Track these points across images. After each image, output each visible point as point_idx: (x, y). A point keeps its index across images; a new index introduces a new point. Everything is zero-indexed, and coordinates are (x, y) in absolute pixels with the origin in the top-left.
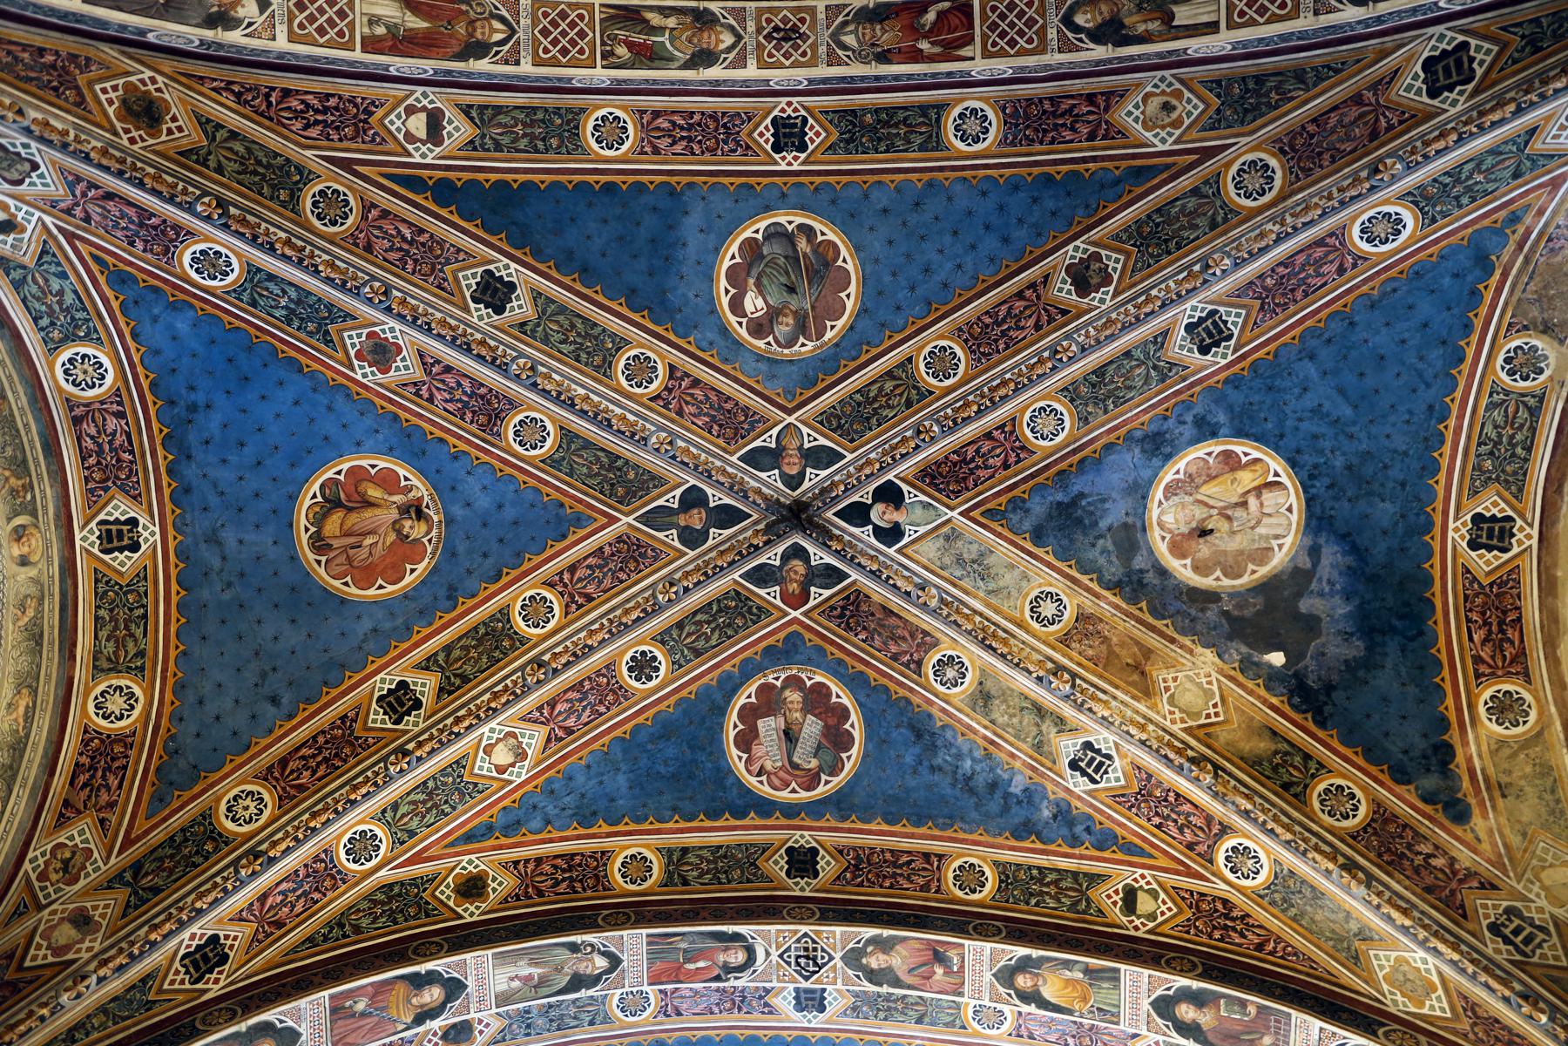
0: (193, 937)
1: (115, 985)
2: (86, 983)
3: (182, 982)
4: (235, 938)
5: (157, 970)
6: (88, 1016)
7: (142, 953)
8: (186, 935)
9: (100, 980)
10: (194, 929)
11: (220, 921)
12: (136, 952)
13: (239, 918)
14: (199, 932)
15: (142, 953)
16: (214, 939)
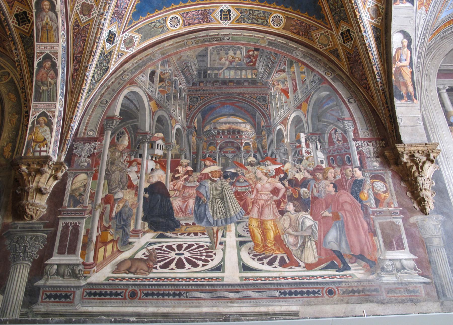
0: (13, 22)
1: (20, 46)
2: (14, 53)
3: (28, 26)
4: (19, 8)
5: (20, 33)
6: (26, 53)
7: (12, 37)
8: (11, 24)
9: (16, 49)
10: (10, 21)
11: (10, 13)
12: (11, 39)
13: (11, 7)
14: (12, 20)
15: (12, 37)
16: (16, 16)
